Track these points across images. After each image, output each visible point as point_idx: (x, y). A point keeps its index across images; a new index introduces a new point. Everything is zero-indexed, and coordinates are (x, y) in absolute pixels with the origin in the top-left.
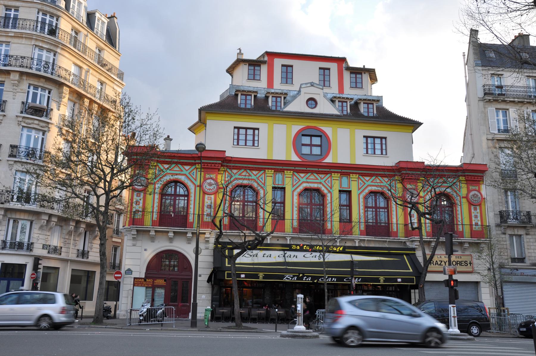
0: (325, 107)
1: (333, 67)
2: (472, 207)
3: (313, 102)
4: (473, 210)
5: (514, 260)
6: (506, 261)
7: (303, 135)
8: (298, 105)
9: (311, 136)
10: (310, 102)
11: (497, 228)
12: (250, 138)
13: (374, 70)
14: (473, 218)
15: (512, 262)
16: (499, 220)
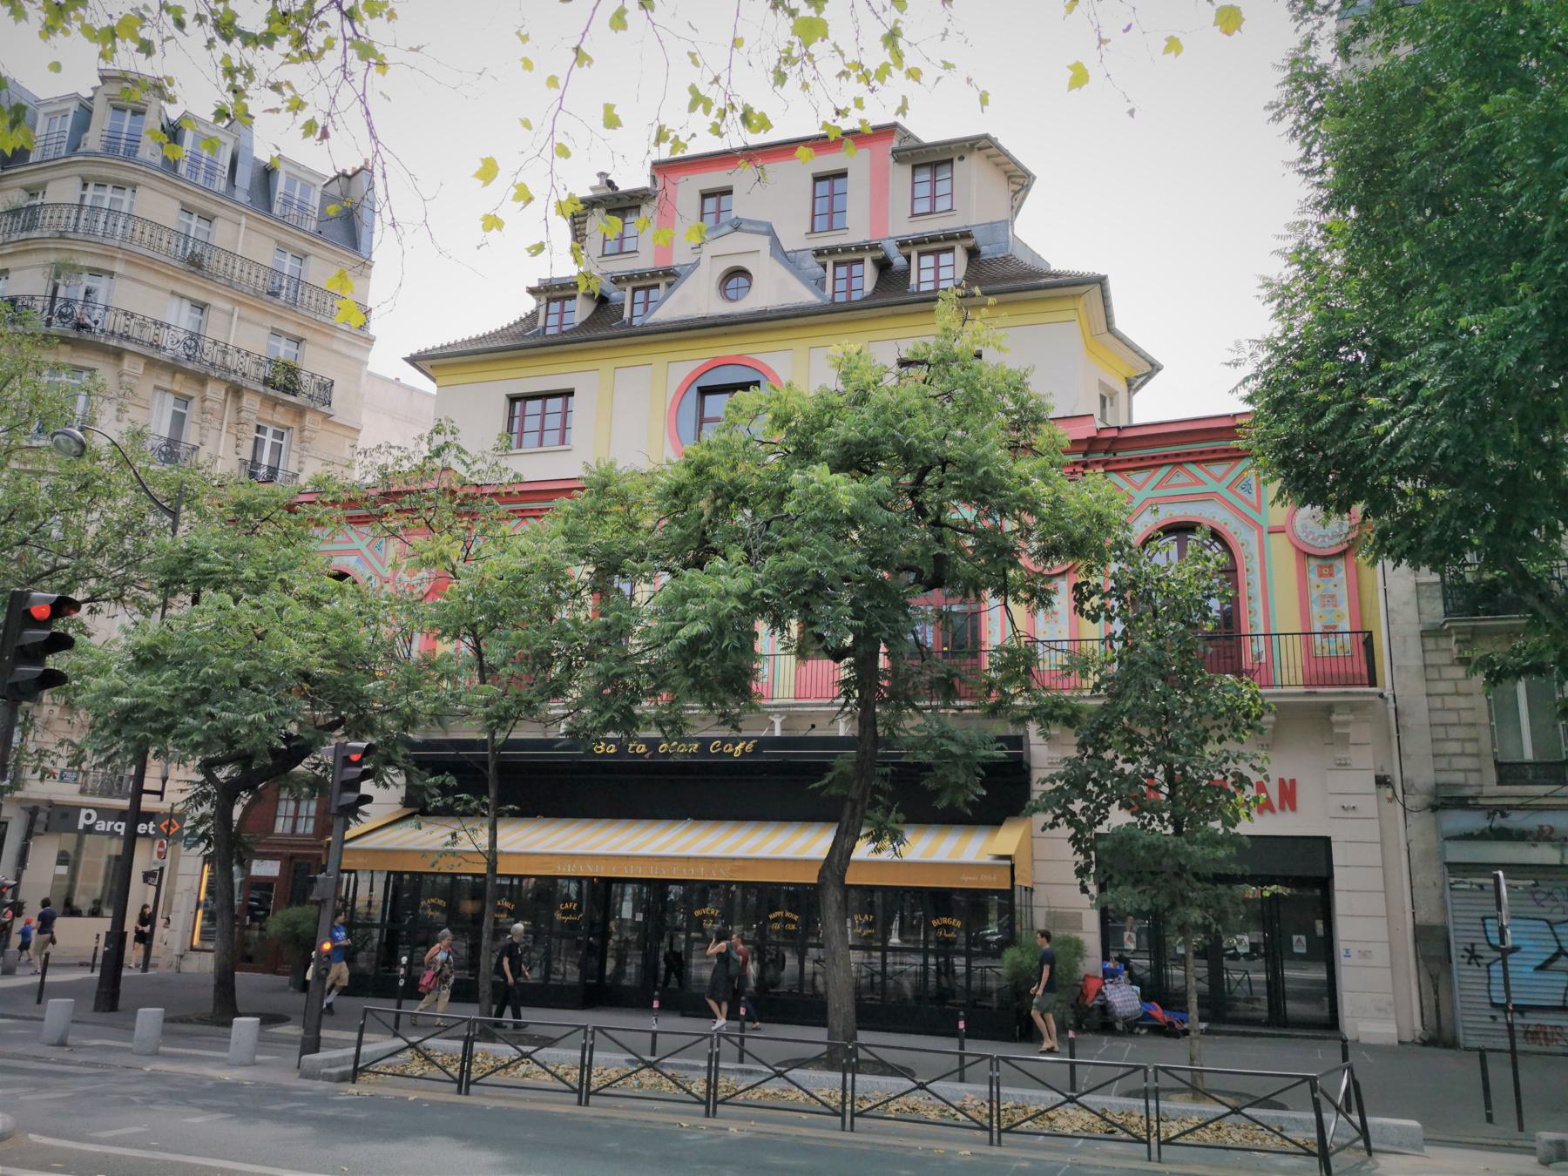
0: (774, 288)
1: (856, 161)
2: (1313, 563)
3: (742, 281)
4: (1313, 577)
5: (1508, 772)
6: (1473, 778)
7: (704, 391)
8: (696, 298)
9: (730, 389)
10: (733, 283)
11: (1430, 643)
12: (553, 421)
13: (986, 137)
14: (1316, 610)
15: (1499, 783)
16: (1441, 609)
